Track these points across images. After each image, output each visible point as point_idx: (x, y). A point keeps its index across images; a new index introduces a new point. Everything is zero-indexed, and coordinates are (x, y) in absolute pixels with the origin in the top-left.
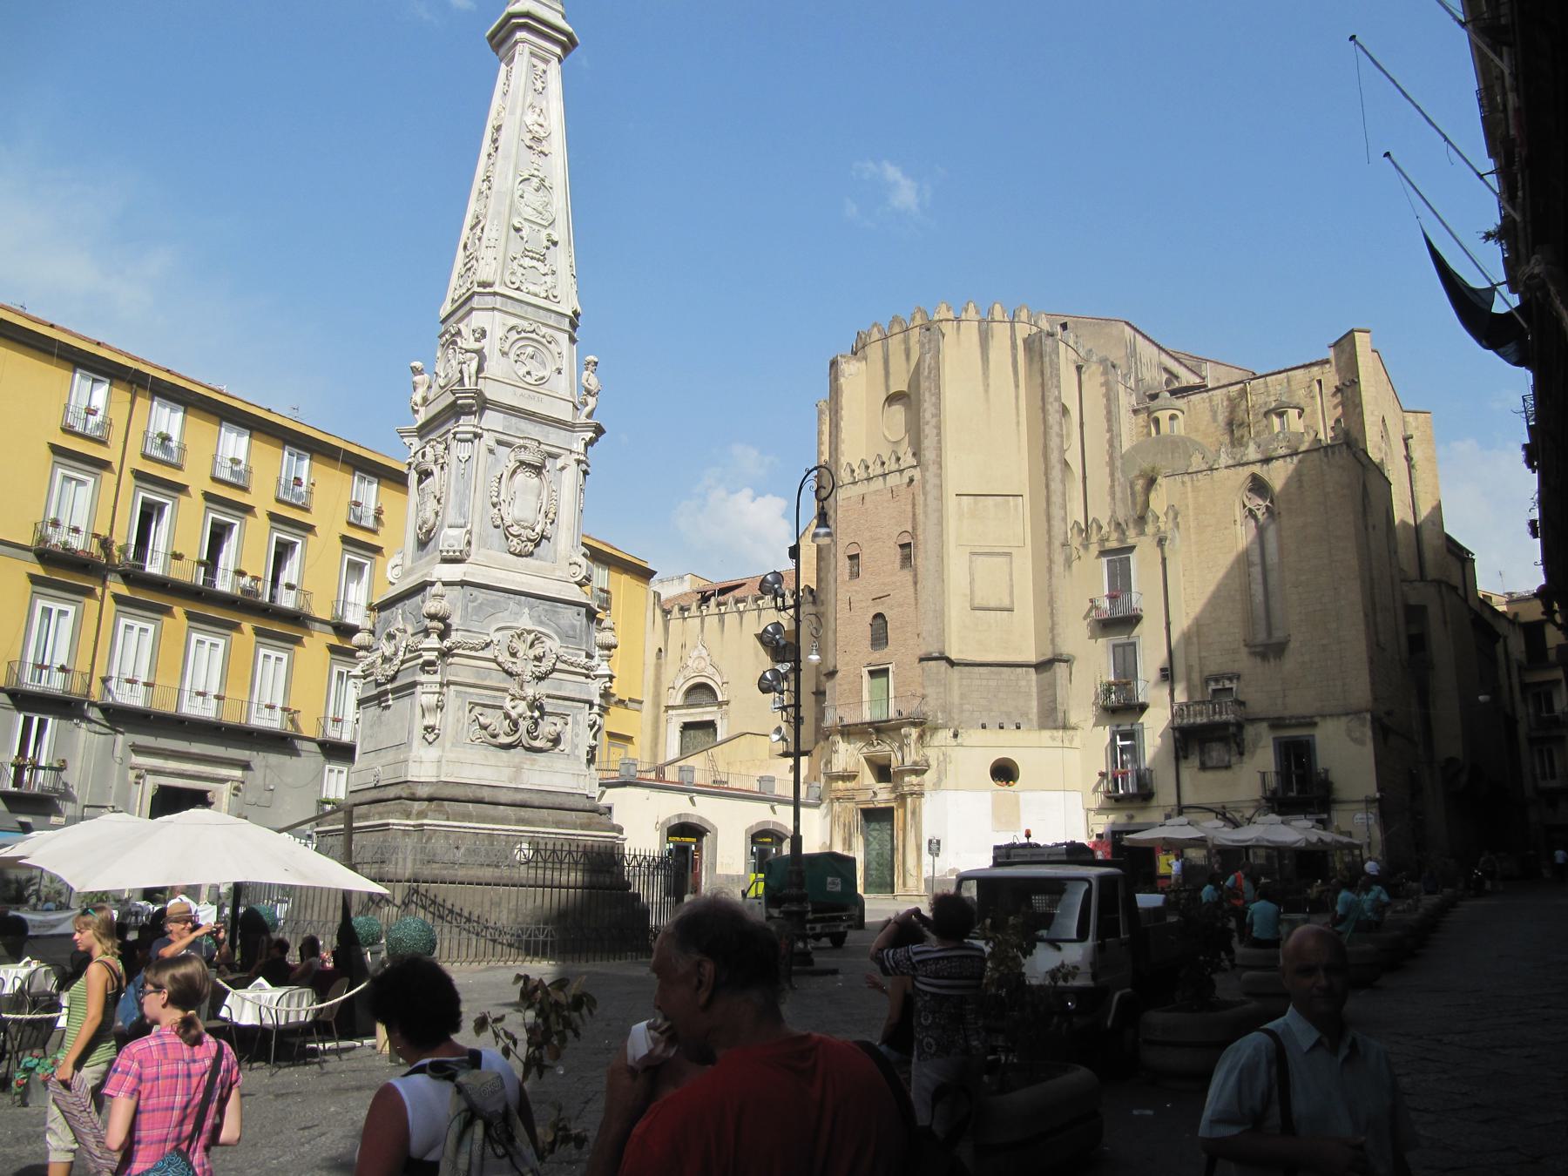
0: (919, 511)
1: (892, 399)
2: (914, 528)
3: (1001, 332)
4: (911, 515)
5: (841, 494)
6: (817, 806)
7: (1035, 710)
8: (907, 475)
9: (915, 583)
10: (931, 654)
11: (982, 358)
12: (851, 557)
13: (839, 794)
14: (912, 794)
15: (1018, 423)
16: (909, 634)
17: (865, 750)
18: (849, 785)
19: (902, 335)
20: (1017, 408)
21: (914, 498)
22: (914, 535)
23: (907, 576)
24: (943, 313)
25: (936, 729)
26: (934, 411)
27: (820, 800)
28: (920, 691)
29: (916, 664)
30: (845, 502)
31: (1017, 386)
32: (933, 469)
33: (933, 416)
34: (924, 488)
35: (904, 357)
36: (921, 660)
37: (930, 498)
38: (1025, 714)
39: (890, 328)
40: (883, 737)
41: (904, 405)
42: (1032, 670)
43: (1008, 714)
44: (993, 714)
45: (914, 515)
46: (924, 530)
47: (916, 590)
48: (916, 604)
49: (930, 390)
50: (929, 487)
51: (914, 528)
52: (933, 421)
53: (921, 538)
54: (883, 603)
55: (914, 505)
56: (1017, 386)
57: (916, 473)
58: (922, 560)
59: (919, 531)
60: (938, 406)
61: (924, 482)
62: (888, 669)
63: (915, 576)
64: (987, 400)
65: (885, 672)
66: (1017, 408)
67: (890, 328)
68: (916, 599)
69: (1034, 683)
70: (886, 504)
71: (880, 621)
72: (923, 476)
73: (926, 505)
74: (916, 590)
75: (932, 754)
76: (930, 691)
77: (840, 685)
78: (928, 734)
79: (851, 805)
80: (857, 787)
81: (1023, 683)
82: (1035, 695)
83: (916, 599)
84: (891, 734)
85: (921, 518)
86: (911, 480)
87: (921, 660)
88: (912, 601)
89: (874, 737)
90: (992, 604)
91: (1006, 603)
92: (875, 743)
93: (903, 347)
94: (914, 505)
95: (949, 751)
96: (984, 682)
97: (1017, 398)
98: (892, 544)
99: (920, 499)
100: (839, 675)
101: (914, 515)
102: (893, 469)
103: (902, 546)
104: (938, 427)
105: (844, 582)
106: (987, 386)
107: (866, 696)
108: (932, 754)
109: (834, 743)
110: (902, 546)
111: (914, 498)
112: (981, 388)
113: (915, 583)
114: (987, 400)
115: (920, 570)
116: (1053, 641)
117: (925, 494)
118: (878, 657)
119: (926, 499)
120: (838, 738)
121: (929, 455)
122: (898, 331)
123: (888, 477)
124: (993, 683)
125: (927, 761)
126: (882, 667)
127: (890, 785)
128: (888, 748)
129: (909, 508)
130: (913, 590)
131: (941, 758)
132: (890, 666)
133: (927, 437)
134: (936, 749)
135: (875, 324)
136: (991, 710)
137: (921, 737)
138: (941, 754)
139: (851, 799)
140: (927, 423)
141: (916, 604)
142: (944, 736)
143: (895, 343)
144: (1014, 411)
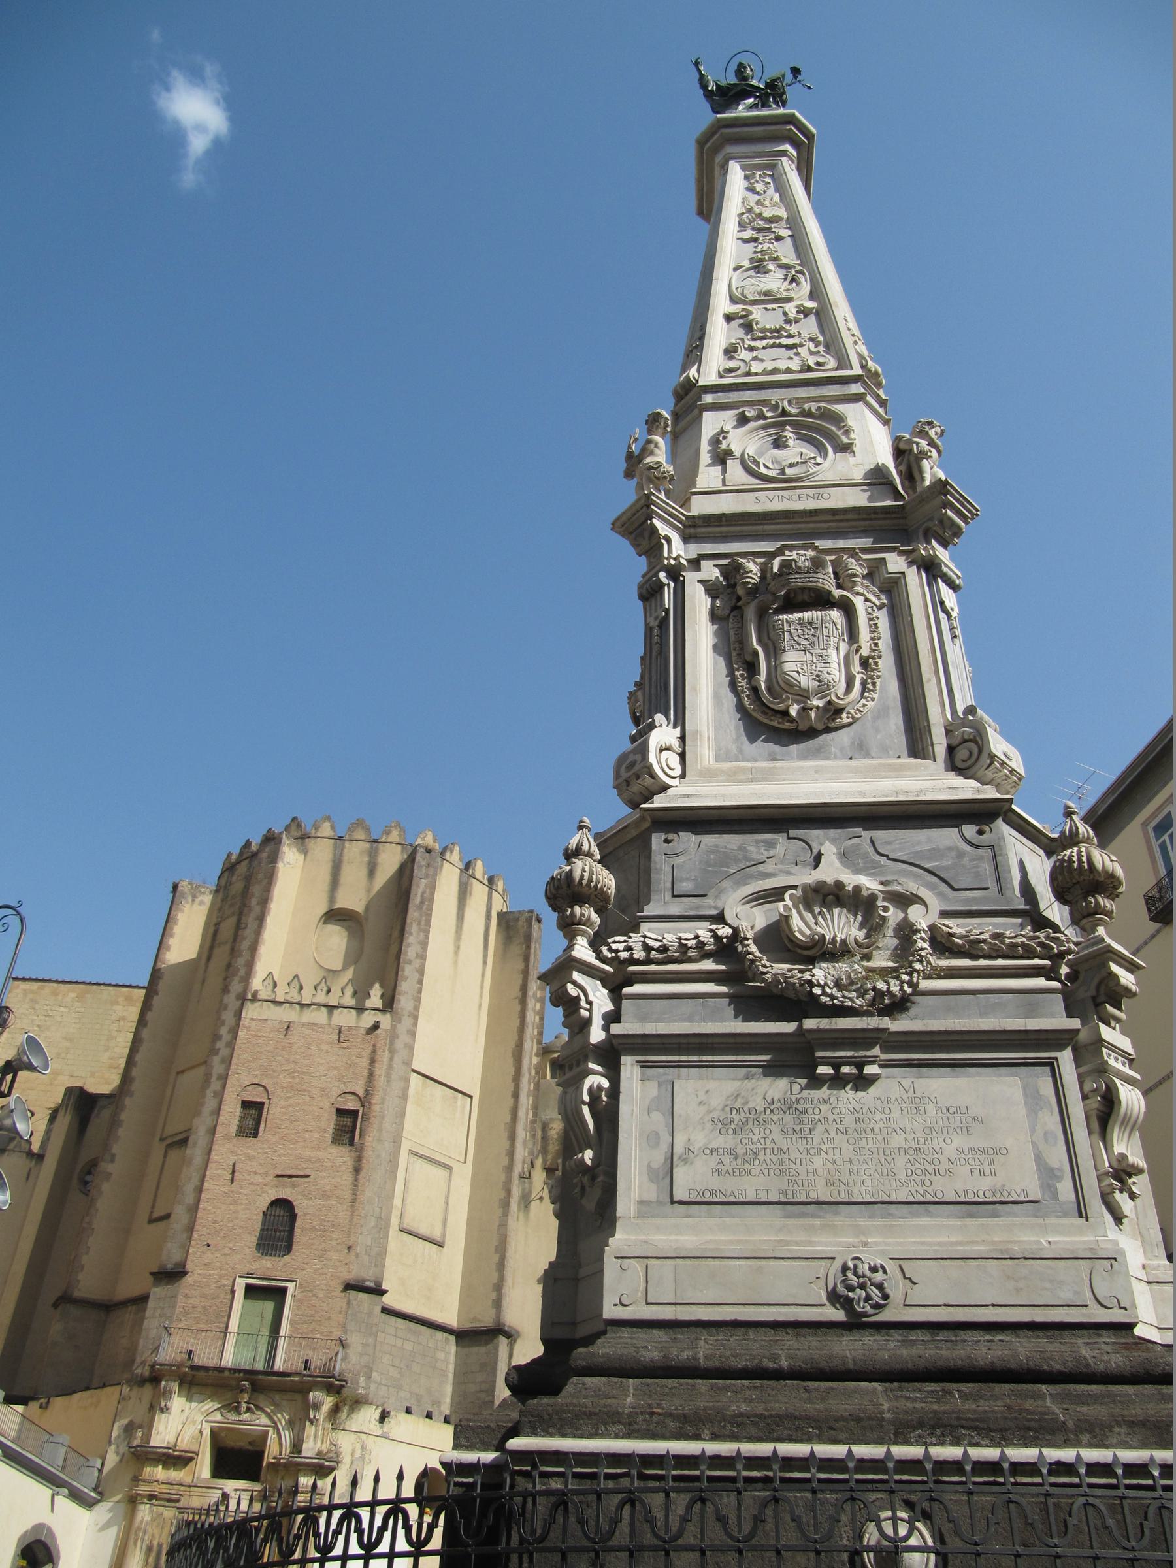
0: (380, 1070)
1: (333, 916)
2: (368, 1093)
3: (479, 892)
4: (365, 1073)
5: (251, 1012)
6: (87, 1503)
7: (448, 1400)
8: (368, 1019)
9: (357, 1170)
10: (364, 1281)
11: (458, 914)
12: (246, 1104)
13: (156, 1489)
14: (151, 1497)
15: (480, 1005)
16: (333, 1243)
17: (218, 1417)
18: (175, 1475)
19: (367, 845)
20: (482, 988)
21: (374, 1052)
22: (365, 1100)
23: (342, 1156)
24: (428, 839)
25: (358, 1403)
26: (420, 950)
27: (100, 1493)
28: (337, 1334)
29: (338, 1292)
30: (254, 1024)
31: (485, 963)
32: (406, 1022)
33: (418, 956)
34: (391, 1044)
35: (364, 872)
36: (349, 1287)
37: (397, 1059)
38: (437, 1403)
39: (351, 830)
40: (262, 1400)
41: (347, 929)
42: (452, 1339)
43: (419, 1399)
44: (402, 1394)
45: (371, 1074)
46: (383, 1099)
47: (356, 1180)
48: (354, 1201)
49: (419, 924)
50: (399, 1044)
51: (368, 1093)
52: (417, 963)
53: (376, 1108)
54: (294, 1186)
55: (373, 1061)
56: (485, 963)
57: (385, 1020)
58: (373, 1140)
59: (376, 1099)
60: (424, 945)
61: (393, 1036)
62: (284, 1291)
63: (359, 1160)
64: (456, 963)
65: (278, 1294)
66: (482, 988)
67: (351, 830)
68: (354, 1194)
69: (452, 1359)
70: (324, 1047)
71: (279, 1212)
72: (393, 1027)
73: (390, 1067)
74: (356, 1180)
75: (346, 1443)
76: (354, 1339)
77: (186, 1296)
78: (345, 1410)
79: (169, 1513)
80: (188, 1480)
81: (441, 1355)
82: (451, 1376)
83: (354, 1194)
84: (277, 1397)
85: (381, 1081)
86: (376, 1026)
87: (349, 1287)
88: (348, 1195)
89: (246, 1397)
90: (423, 1230)
91: (437, 1235)
92: (243, 1409)
93: (366, 859)
94: (373, 1061)
95: (370, 1442)
96: (399, 1343)
97: (483, 976)
98: (326, 1104)
99: (384, 1057)
100: (188, 1279)
101: (371, 1074)
102: (346, 1004)
103: (340, 1112)
104: (421, 972)
105: (227, 1137)
106: (457, 948)
107: (234, 1326)
108: (346, 1443)
109: (167, 1394)
110: (340, 1112)
111: (374, 1052)
112: (451, 948)
113: (357, 1170)
114: (456, 963)
115: (368, 1154)
116: (498, 1304)
117: (392, 1051)
118: (270, 1267)
119: (391, 1059)
120: (175, 1386)
121: (404, 1003)
122: (362, 838)
123: (336, 1012)
124: (408, 1346)
125: (338, 1454)
126: (274, 1283)
127: (257, 1487)
128: (264, 1420)
129: (364, 1062)
130: (351, 1179)
131: (358, 1454)
132: (291, 1287)
133: (406, 979)
134: (353, 1436)
135: (328, 818)
136: (400, 1388)
137: (336, 1410)
138: (358, 1446)
139: (171, 1501)
140: (410, 962)
141: (354, 1201)
142: (367, 1417)
143: (355, 852)
144: (478, 990)
